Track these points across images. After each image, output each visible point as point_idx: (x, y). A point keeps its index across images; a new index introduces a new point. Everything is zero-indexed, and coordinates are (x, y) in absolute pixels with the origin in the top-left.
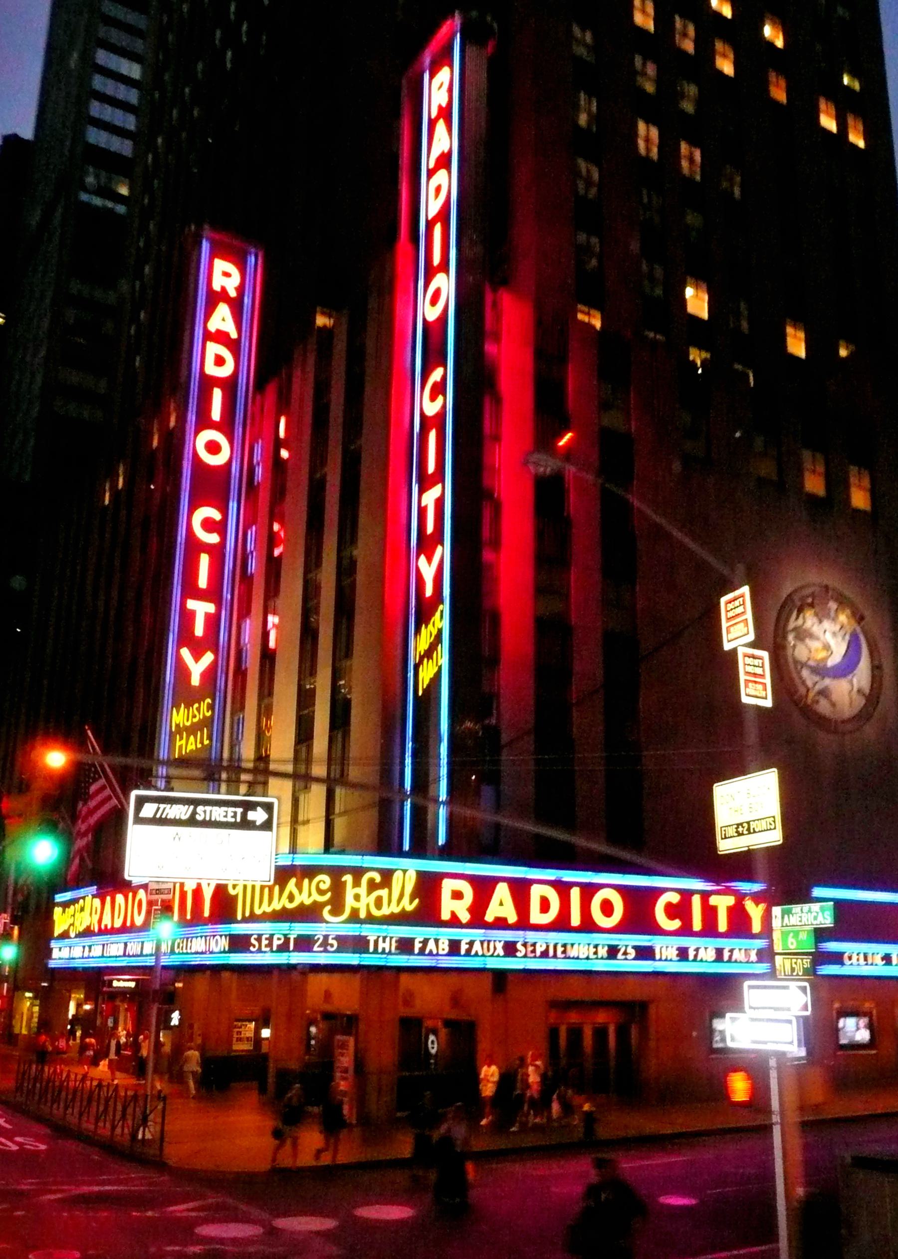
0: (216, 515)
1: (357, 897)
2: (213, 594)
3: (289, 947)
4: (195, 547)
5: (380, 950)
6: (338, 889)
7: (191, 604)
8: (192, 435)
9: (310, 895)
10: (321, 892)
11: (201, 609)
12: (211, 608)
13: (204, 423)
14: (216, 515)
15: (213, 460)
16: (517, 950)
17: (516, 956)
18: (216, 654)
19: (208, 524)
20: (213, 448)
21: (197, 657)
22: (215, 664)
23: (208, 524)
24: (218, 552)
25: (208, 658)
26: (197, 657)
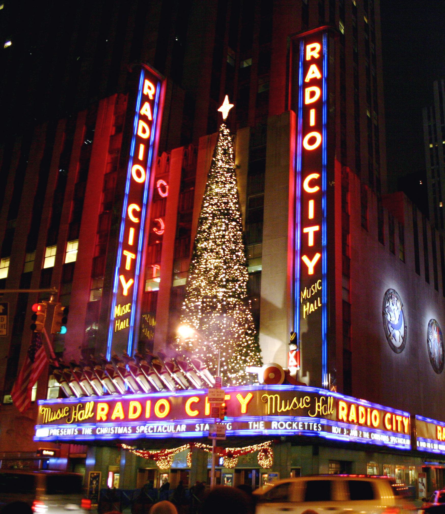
0: (138, 209)
1: (319, 406)
2: (134, 249)
3: (249, 427)
4: (129, 224)
5: (254, 428)
6: (312, 403)
7: (126, 253)
8: (131, 166)
9: (303, 405)
10: (307, 403)
11: (130, 256)
12: (133, 256)
13: (136, 161)
14: (138, 209)
15: (140, 180)
16: (195, 428)
17: (195, 431)
18: (134, 279)
19: (135, 213)
20: (139, 174)
21: (127, 281)
22: (133, 285)
23: (135, 213)
24: (137, 227)
25: (131, 281)
26: (127, 281)
